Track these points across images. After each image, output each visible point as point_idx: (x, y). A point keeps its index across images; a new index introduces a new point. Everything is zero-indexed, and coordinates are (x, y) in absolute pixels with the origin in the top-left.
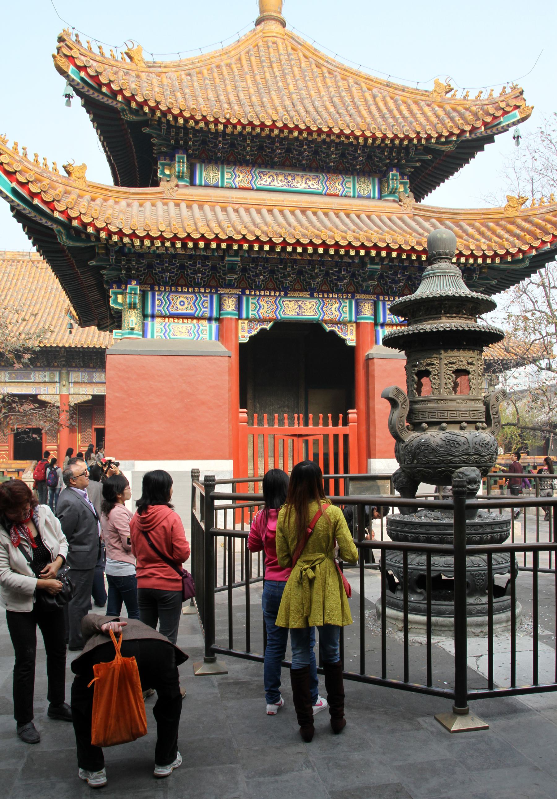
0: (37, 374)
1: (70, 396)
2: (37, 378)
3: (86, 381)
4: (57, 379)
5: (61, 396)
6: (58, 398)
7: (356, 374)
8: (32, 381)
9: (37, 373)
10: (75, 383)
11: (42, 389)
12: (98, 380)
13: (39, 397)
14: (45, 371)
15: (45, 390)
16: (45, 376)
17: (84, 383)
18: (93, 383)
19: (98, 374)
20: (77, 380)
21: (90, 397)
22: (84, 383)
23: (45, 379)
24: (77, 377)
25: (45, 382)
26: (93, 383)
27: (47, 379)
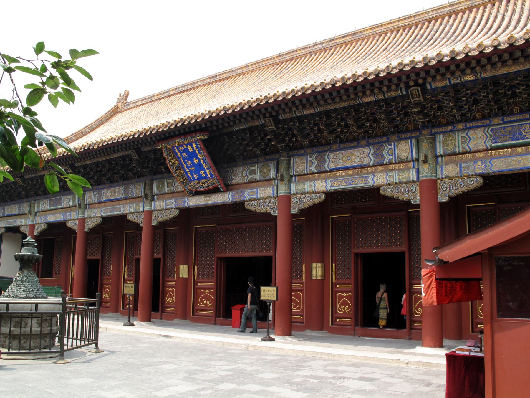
1: (86, 220)
10: (91, 204)
16: (70, 200)
17: (96, 203)
18: (102, 202)
21: (100, 220)
22: (96, 203)
24: (90, 197)
25: (70, 207)
26: (102, 202)
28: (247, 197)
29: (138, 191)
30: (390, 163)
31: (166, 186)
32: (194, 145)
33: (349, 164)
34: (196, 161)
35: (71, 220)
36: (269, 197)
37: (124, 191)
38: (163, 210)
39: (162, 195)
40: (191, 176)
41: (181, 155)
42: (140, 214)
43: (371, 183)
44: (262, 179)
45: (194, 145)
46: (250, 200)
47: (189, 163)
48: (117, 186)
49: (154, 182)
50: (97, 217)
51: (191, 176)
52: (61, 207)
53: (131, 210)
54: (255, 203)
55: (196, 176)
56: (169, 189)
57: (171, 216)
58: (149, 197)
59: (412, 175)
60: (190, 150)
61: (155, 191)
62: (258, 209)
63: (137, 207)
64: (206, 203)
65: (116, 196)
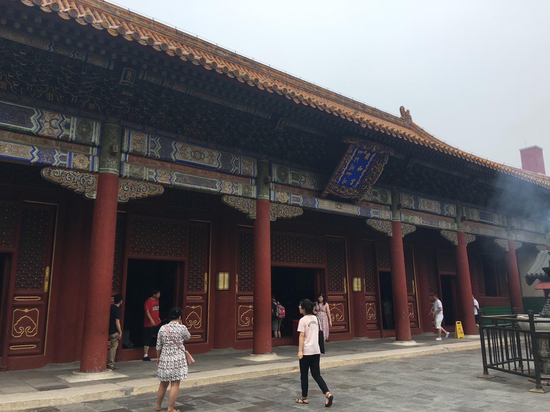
0: (47, 117)
2: (47, 126)
3: (158, 155)
4: (95, 138)
5: (102, 178)
6: (92, 179)
7: (349, 214)
8: (33, 129)
9: (47, 116)
10: (134, 154)
11: (57, 155)
12: (179, 157)
13: (44, 172)
14: (69, 115)
15: (63, 158)
16: (67, 126)
17: (153, 158)
18: (170, 161)
19: (179, 145)
20: (138, 148)
23: (66, 132)
24: (139, 142)
25: (65, 139)
27: (72, 134)
28: (372, 215)
29: (247, 169)
30: (446, 216)
31: (290, 176)
32: (374, 155)
33: (430, 210)
34: (360, 169)
35: (69, 169)
36: (387, 220)
37: (222, 159)
38: (286, 204)
39: (283, 185)
40: (340, 180)
41: (354, 158)
42: (249, 200)
43: (440, 227)
44: (383, 202)
45: (374, 155)
46: (374, 218)
47: (353, 167)
48: (206, 146)
49: (273, 165)
50: (157, 183)
51: (340, 180)
52: (28, 129)
53: (235, 191)
54: (376, 221)
55: (345, 181)
56: (294, 181)
57: (296, 215)
58: (262, 181)
59: (455, 227)
60: (367, 158)
61: (275, 177)
62: (379, 228)
63: (247, 190)
64: (337, 210)
65: (205, 162)
